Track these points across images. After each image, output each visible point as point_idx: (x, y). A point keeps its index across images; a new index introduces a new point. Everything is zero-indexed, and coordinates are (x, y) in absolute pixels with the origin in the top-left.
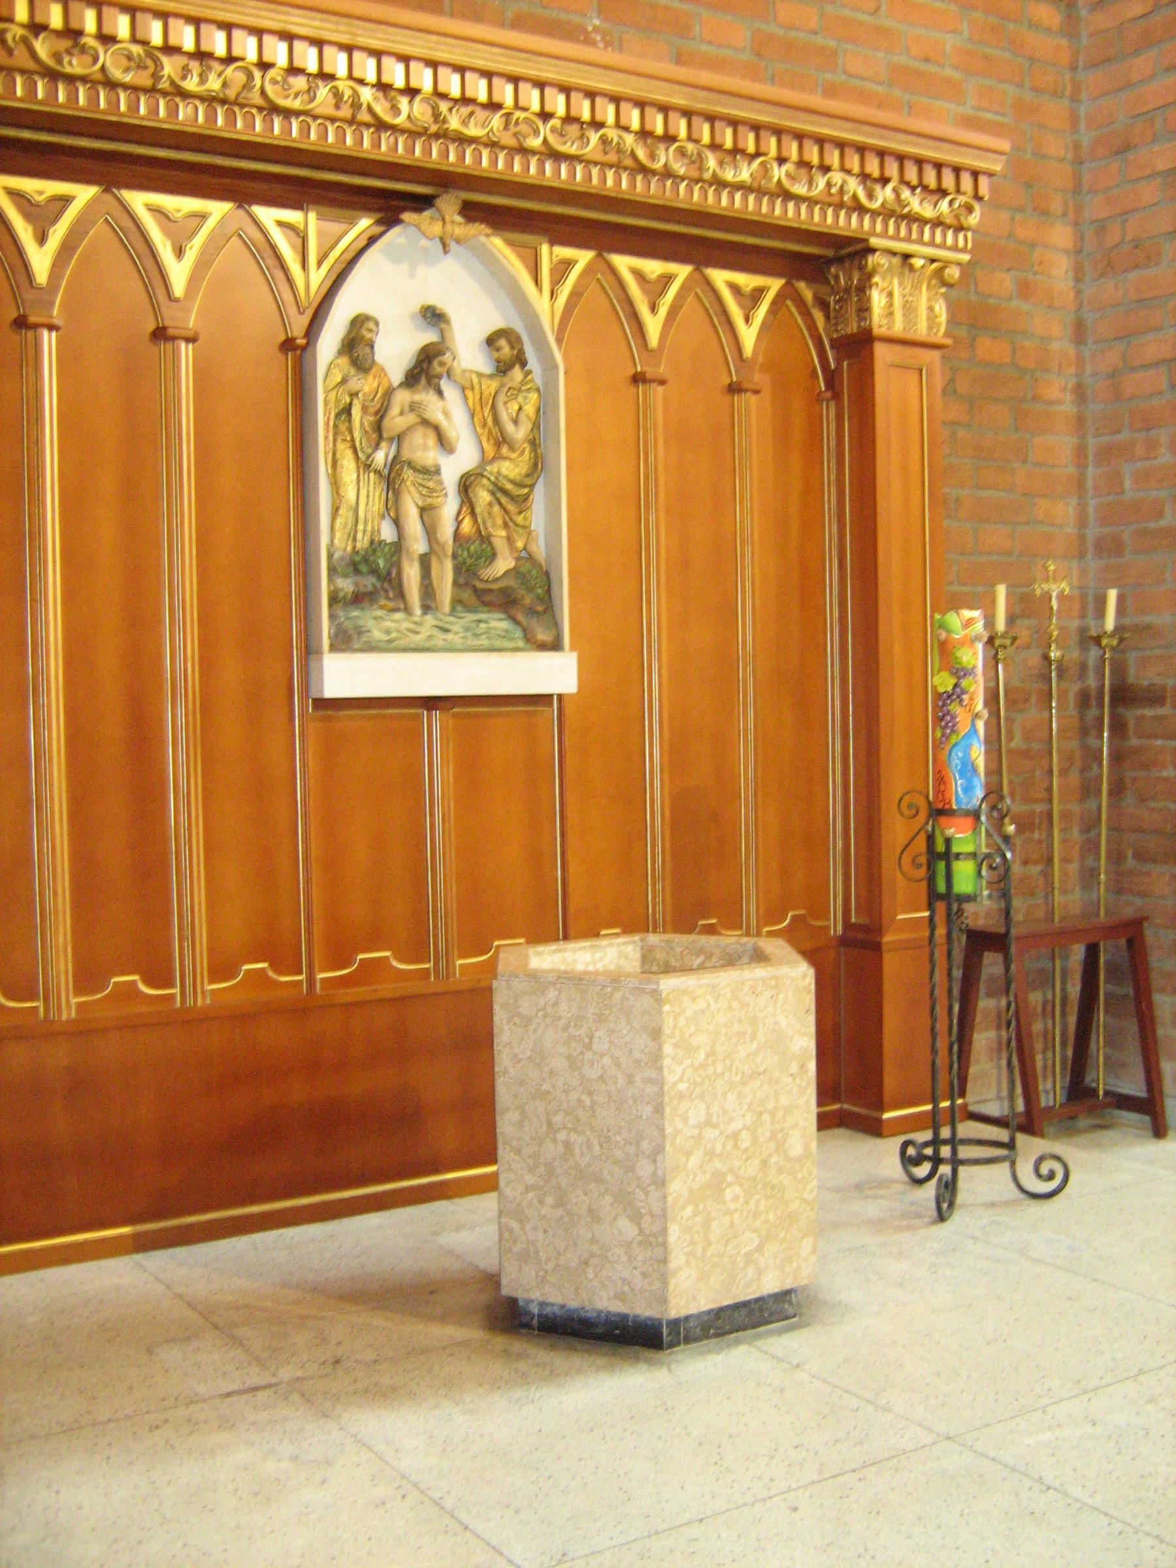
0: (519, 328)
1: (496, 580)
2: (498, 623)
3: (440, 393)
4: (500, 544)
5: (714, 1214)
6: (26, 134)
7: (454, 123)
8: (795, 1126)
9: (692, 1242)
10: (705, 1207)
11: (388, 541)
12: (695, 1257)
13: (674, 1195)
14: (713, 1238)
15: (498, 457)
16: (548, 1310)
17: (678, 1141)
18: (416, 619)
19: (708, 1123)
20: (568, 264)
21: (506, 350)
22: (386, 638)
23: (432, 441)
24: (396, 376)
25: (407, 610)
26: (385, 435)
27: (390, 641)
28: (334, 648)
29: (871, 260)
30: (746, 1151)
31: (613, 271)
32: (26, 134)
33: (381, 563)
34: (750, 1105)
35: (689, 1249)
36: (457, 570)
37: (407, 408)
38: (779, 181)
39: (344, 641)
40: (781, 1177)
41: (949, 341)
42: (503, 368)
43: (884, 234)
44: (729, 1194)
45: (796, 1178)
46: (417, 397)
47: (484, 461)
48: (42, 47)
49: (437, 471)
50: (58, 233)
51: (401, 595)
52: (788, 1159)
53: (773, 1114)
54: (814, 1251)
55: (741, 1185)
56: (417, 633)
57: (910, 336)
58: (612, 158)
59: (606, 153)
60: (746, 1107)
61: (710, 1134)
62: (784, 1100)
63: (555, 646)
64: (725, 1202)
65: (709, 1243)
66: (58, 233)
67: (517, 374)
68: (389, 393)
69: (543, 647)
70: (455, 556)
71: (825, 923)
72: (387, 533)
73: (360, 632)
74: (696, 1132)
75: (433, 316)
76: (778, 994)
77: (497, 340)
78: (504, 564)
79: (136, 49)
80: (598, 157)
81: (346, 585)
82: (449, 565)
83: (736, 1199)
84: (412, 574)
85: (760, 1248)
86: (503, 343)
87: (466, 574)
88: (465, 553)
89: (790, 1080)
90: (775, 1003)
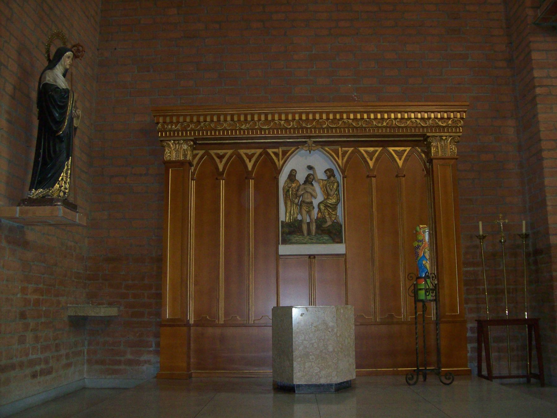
0: (333, 167)
1: (324, 228)
2: (326, 237)
3: (312, 185)
4: (328, 220)
5: (306, 362)
6: (227, 141)
7: (304, 125)
8: (330, 344)
9: (300, 367)
10: (304, 359)
11: (299, 220)
12: (301, 371)
13: (295, 355)
14: (306, 367)
15: (328, 198)
16: (282, 384)
17: (296, 343)
18: (305, 237)
19: (305, 340)
20: (346, 152)
21: (329, 173)
22: (296, 241)
23: (309, 196)
24: (302, 181)
25: (303, 235)
26: (298, 196)
27: (297, 242)
28: (282, 244)
29: (429, 140)
30: (316, 348)
31: (360, 151)
32: (227, 141)
33: (296, 225)
34: (317, 337)
35: (300, 368)
36: (317, 225)
37: (303, 189)
38: (375, 124)
39: (285, 242)
40: (326, 356)
41: (458, 157)
42: (329, 177)
43: (432, 132)
44: (311, 357)
45: (331, 356)
46: (306, 186)
47: (325, 199)
48: (213, 125)
49: (311, 203)
50: (224, 160)
51: (302, 232)
52: (328, 351)
53: (323, 340)
54: (336, 375)
55: (314, 356)
56: (304, 240)
57: (444, 157)
58: (347, 126)
59: (345, 125)
60: (316, 337)
61: (305, 342)
62: (327, 337)
63: (341, 242)
64: (310, 359)
65: (305, 368)
66: (224, 160)
67: (332, 178)
68: (299, 187)
69: (338, 243)
70: (316, 222)
71: (431, 317)
72: (299, 218)
73: (290, 240)
74: (302, 341)
75: (310, 168)
76: (325, 311)
77: (326, 171)
78: (329, 223)
79: (231, 122)
80: (343, 126)
81: (287, 230)
82: (314, 224)
83: (313, 359)
84: (305, 227)
85: (320, 372)
86: (328, 172)
87: (318, 227)
88: (319, 221)
89: (329, 333)
90: (324, 314)
